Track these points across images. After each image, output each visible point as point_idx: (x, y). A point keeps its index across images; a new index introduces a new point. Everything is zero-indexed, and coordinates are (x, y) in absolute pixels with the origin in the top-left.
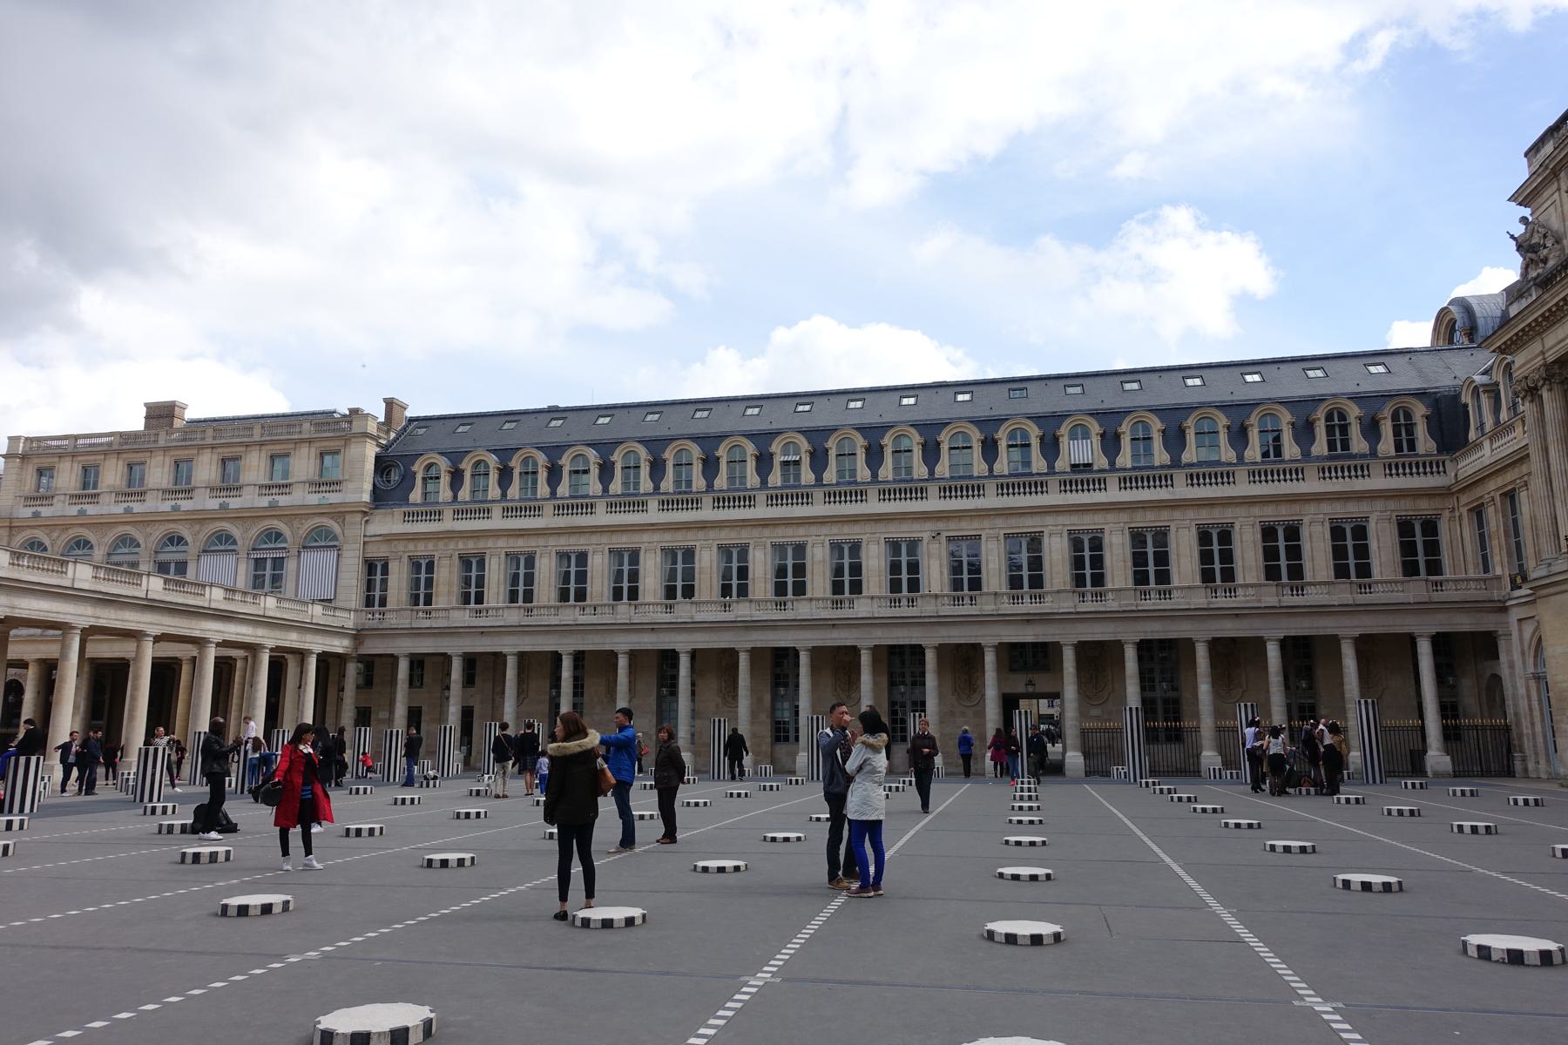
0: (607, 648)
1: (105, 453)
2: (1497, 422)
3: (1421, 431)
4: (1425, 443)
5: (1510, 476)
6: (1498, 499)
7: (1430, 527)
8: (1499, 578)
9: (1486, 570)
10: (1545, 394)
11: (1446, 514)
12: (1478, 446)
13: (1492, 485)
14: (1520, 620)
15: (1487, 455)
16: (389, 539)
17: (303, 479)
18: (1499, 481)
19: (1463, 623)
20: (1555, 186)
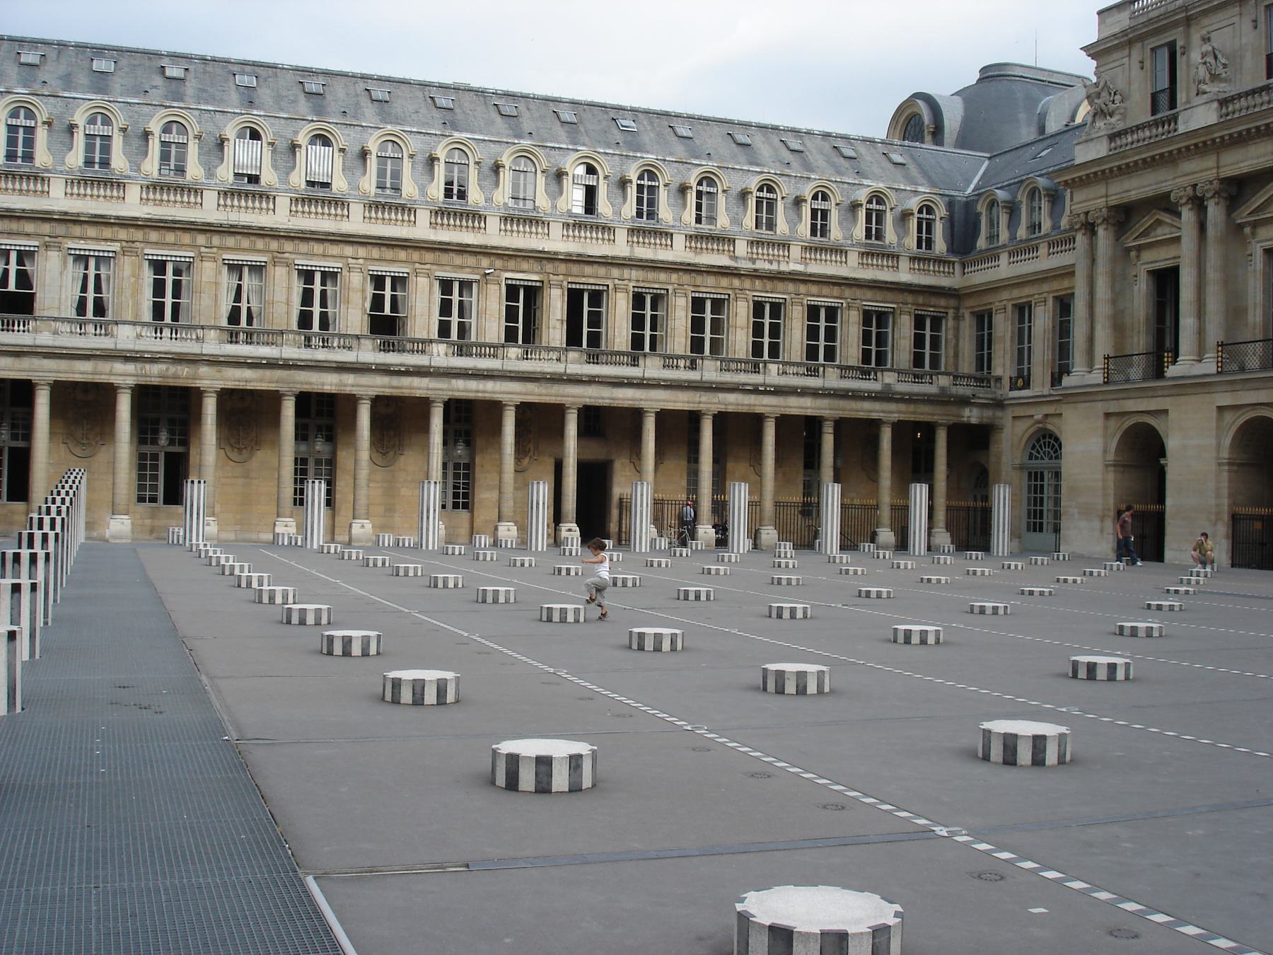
0: (103, 379)
2: (1013, 237)
3: (938, 229)
4: (940, 246)
5: (1027, 291)
6: (1009, 308)
7: (937, 323)
8: (999, 379)
9: (980, 366)
10: (1101, 232)
11: (951, 312)
12: (991, 255)
13: (1005, 295)
14: (1014, 417)
15: (1004, 268)
18: (1016, 293)
19: (972, 416)
20: (1126, 52)
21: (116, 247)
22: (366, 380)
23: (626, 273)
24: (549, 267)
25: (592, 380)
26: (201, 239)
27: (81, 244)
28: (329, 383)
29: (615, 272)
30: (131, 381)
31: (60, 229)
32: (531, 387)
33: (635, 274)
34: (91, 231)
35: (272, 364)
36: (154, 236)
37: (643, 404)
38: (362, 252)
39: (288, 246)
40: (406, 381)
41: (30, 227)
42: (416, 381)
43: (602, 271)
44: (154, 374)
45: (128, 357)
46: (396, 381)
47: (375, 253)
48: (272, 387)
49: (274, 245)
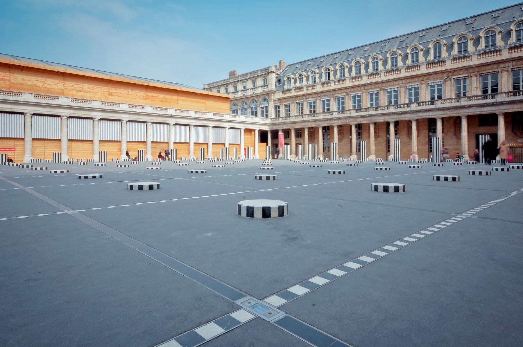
1: (221, 86)
16: (279, 99)
17: (260, 85)
21: (344, 94)
22: (391, 117)
23: (507, 65)
24: (471, 71)
25: (470, 106)
26: (362, 88)
27: (338, 95)
28: (381, 119)
29: (502, 65)
30: (336, 124)
31: (333, 93)
32: (446, 112)
33: (511, 64)
34: (339, 92)
35: (365, 116)
36: (352, 90)
37: (496, 112)
38: (404, 81)
39: (384, 85)
40: (403, 116)
41: (328, 94)
42: (406, 115)
43: (495, 66)
44: (341, 122)
45: (336, 119)
46: (400, 116)
47: (408, 81)
48: (367, 122)
49: (380, 85)
